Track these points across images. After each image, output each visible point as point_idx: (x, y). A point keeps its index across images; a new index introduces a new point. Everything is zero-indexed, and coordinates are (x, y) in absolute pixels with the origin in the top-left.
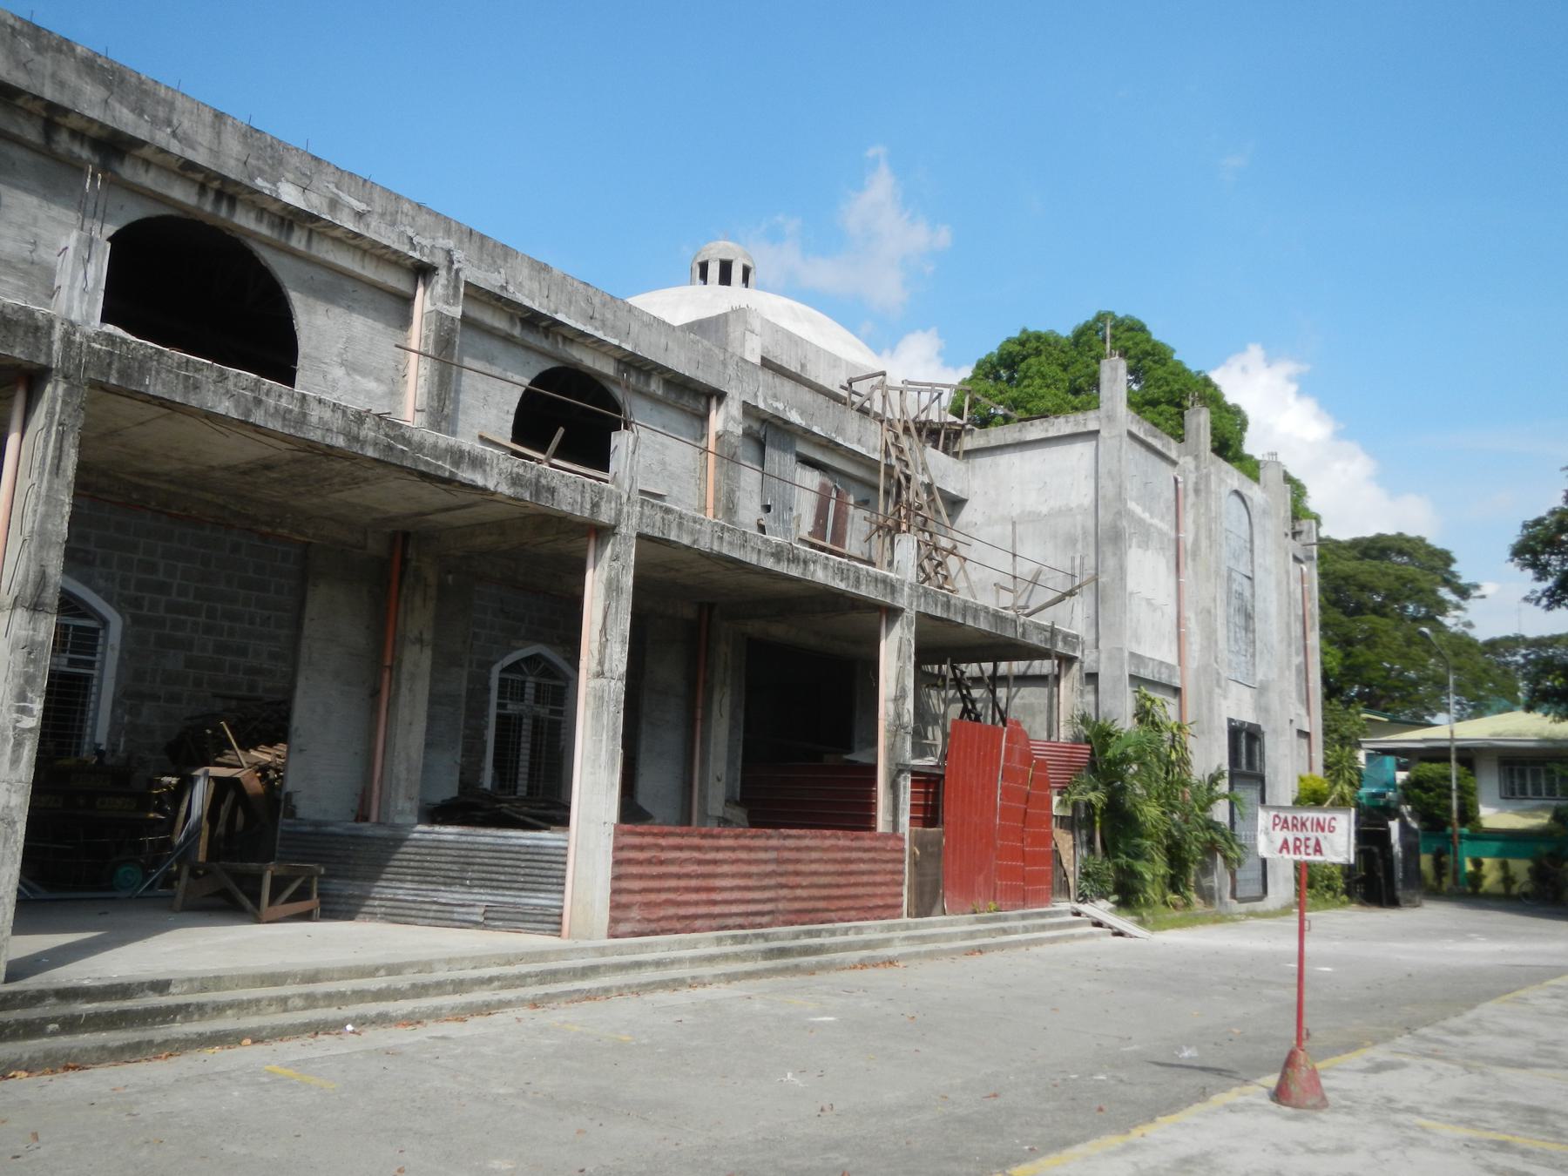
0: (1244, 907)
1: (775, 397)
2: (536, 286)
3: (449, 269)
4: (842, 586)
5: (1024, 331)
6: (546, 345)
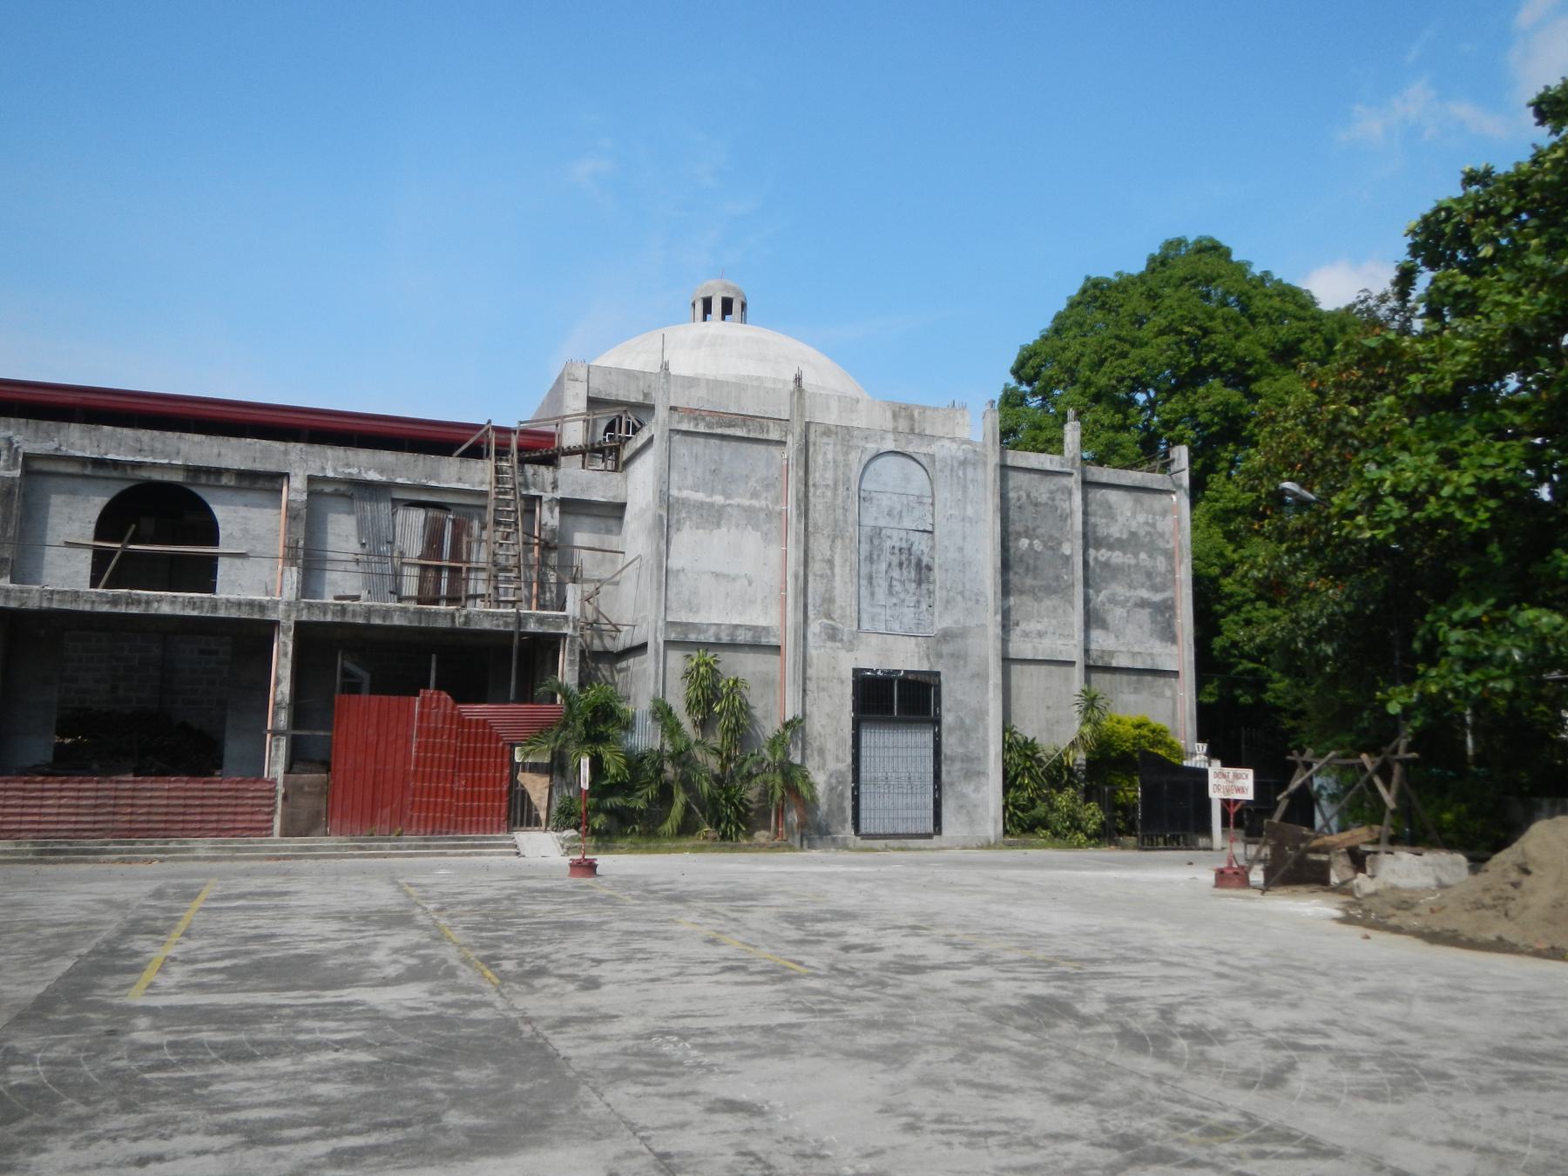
0: (860, 842)
1: (348, 465)
2: (86, 442)
3: (9, 449)
4: (195, 613)
5: (1088, 279)
6: (115, 474)
